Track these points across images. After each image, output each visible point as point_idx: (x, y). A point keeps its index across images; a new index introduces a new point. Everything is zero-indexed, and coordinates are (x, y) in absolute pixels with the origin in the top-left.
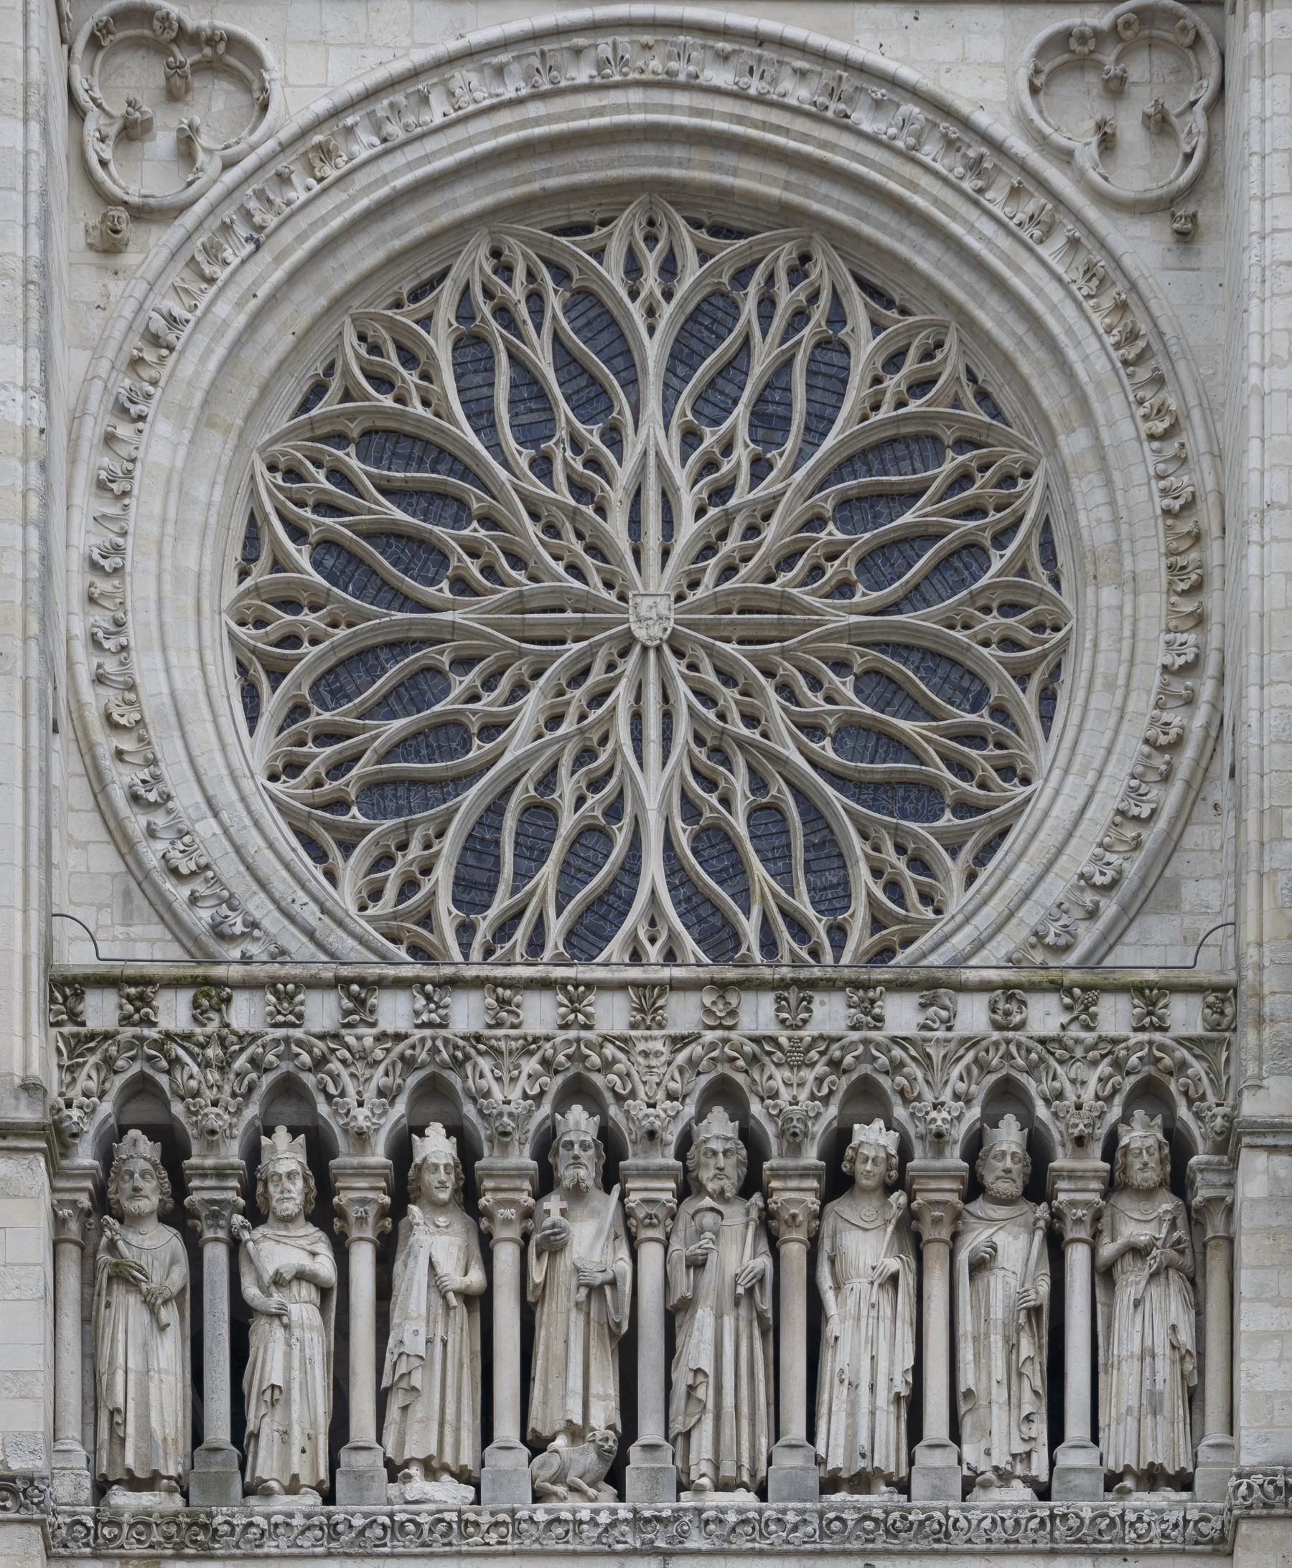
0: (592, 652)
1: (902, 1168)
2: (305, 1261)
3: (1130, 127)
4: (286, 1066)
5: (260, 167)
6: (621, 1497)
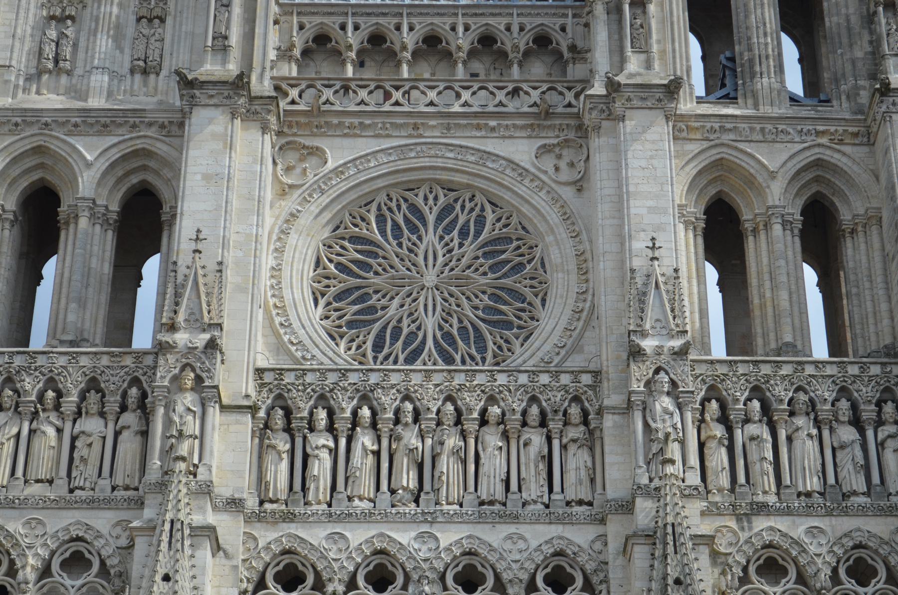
0: (413, 289)
1: (503, 419)
2: (326, 443)
3: (563, 164)
4: (322, 391)
5: (324, 176)
6: (418, 506)
